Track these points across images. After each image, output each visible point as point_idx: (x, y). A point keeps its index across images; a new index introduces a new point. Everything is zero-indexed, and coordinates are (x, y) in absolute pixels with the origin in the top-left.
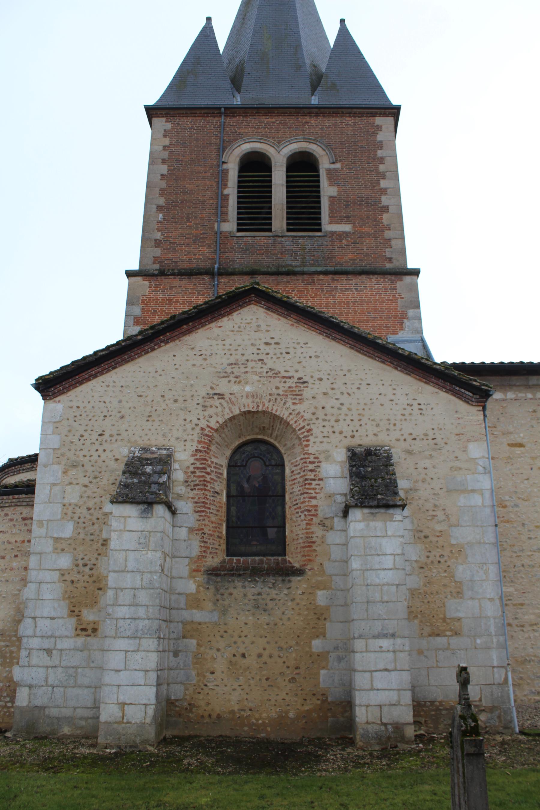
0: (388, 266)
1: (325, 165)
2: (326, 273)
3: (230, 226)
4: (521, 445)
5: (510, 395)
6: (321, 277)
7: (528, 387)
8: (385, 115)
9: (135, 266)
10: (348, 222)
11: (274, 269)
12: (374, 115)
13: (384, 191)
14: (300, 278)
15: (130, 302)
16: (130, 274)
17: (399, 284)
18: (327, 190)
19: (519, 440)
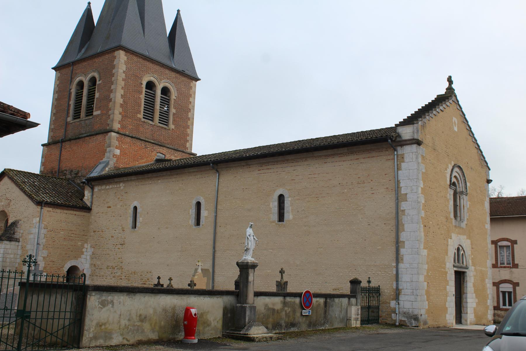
0: (108, 128)
1: (98, 83)
2: (87, 136)
3: (70, 119)
4: (110, 207)
5: (111, 187)
6: (87, 138)
7: (116, 182)
8: (118, 50)
9: (46, 142)
10: (100, 109)
11: (74, 137)
12: (114, 51)
13: (111, 91)
14: (81, 139)
15: (42, 157)
16: (43, 145)
17: (107, 137)
18: (97, 95)
19: (110, 205)
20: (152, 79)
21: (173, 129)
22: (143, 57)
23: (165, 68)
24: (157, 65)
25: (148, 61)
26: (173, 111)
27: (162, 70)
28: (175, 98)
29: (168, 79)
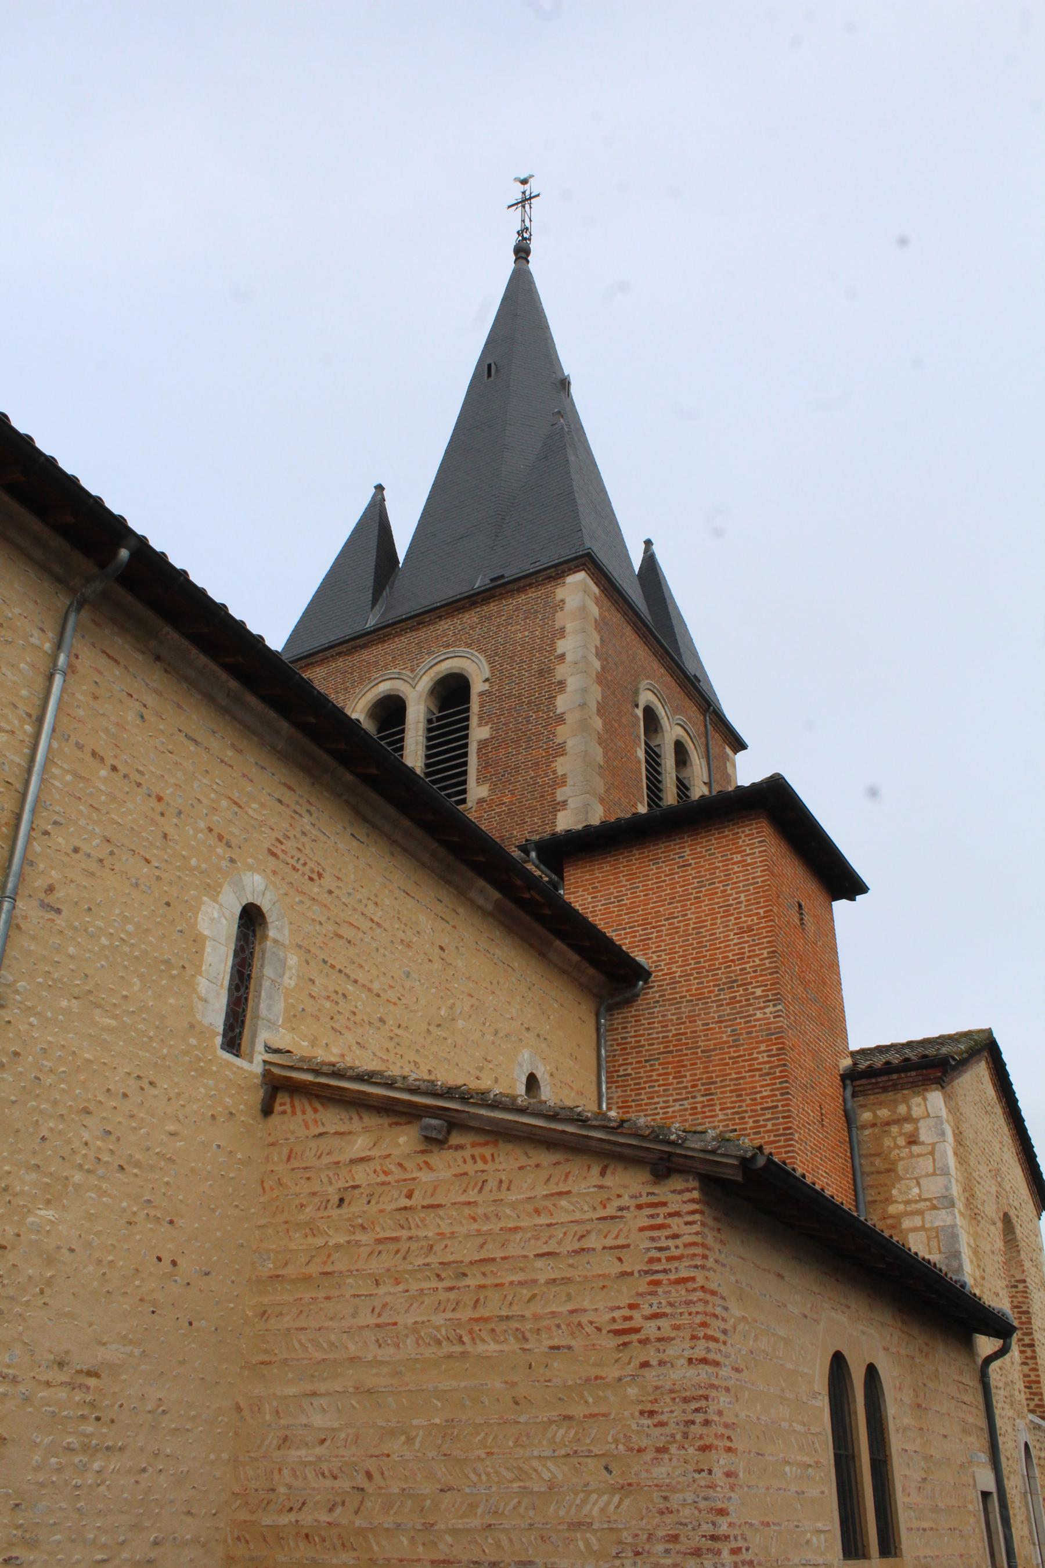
20: (384, 688)
21: (481, 801)
22: (343, 648)
23: (431, 623)
24: (398, 635)
25: (364, 646)
26: (478, 733)
27: (422, 634)
28: (486, 686)
29: (448, 646)
